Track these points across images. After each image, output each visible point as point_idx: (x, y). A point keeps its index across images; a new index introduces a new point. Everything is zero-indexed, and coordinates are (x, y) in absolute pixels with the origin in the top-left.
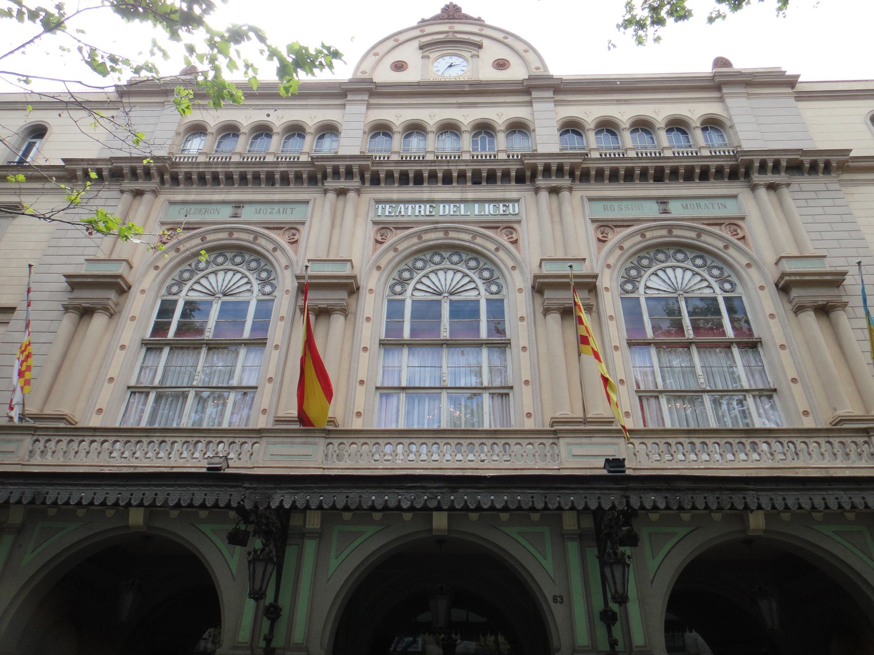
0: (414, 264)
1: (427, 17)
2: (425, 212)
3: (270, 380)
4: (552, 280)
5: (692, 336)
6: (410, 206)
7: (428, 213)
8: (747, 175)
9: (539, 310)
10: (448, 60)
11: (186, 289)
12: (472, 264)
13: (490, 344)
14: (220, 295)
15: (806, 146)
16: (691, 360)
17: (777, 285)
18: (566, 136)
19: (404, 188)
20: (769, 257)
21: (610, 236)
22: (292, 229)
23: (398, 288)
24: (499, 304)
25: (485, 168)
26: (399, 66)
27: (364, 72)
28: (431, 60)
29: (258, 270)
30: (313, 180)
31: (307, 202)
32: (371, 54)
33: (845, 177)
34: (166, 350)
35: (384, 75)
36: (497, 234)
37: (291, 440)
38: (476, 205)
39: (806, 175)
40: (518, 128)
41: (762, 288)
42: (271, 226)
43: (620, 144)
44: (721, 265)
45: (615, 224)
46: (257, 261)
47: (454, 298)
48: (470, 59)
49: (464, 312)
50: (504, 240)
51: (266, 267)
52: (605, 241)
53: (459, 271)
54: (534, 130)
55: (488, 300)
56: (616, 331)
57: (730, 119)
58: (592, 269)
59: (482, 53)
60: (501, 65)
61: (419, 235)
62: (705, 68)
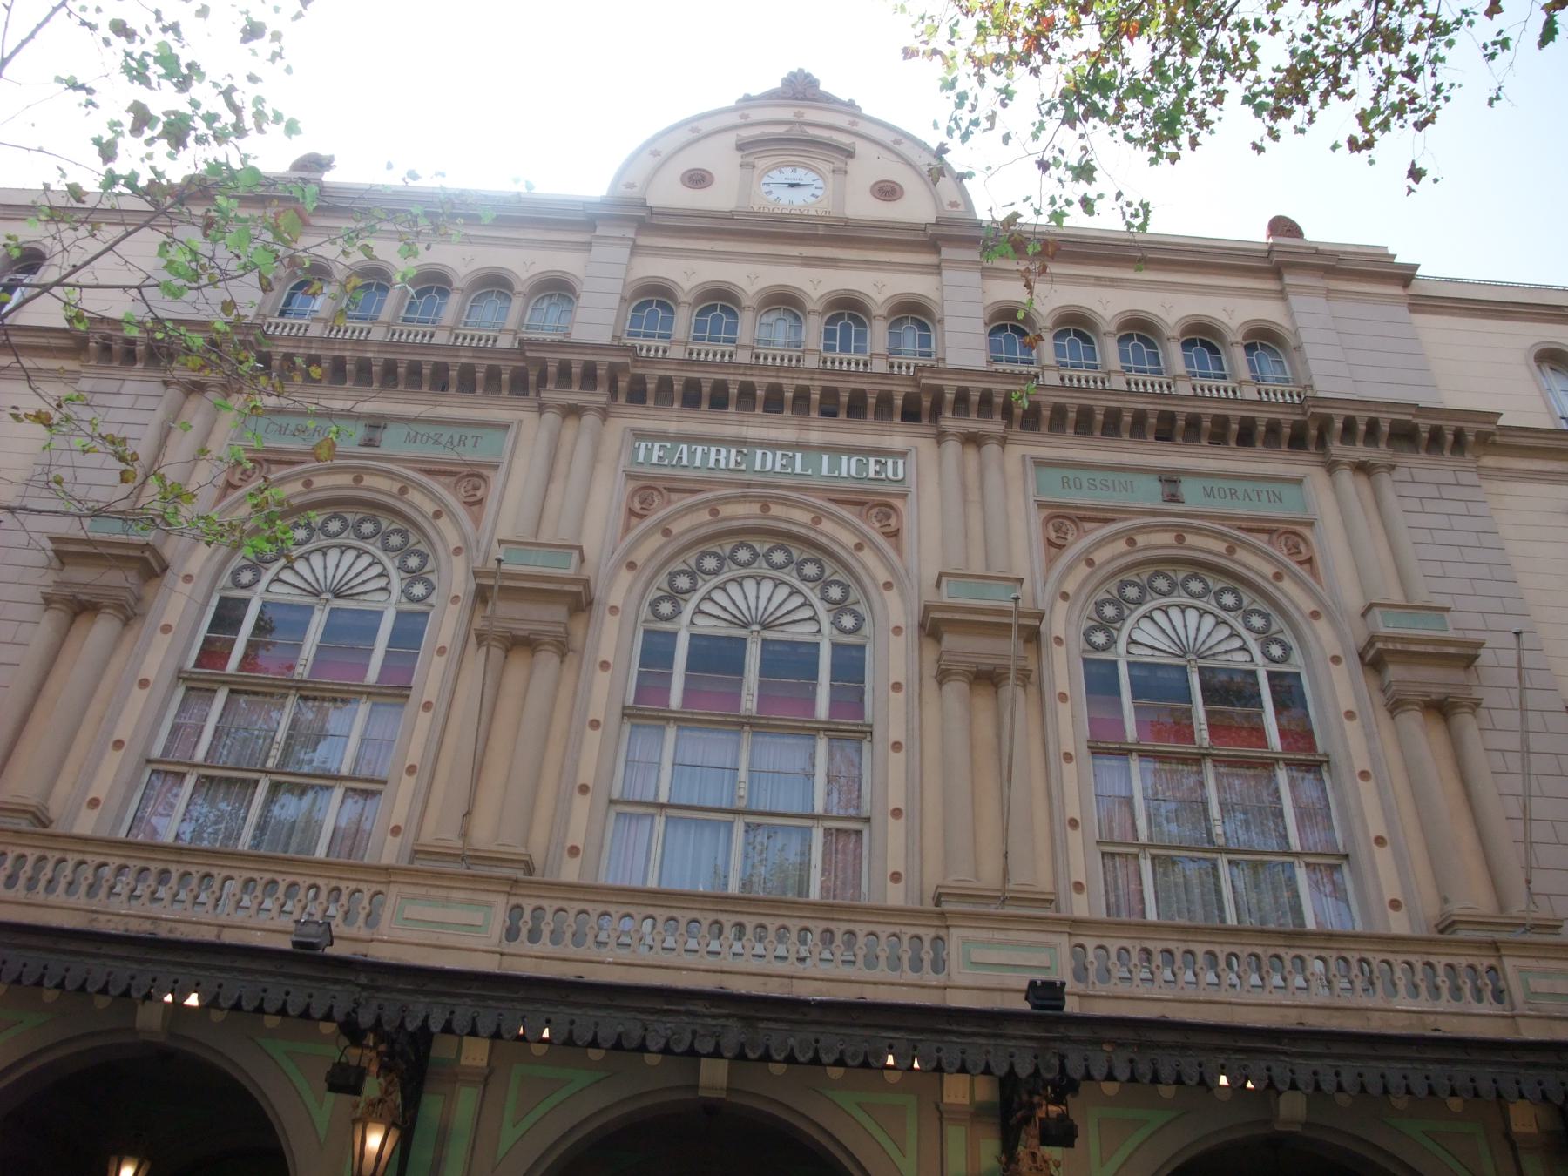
0: (698, 562)
1: (755, 92)
2: (727, 463)
3: (411, 770)
4: (957, 616)
5: (1206, 744)
6: (699, 449)
7: (732, 465)
8: (1322, 442)
9: (930, 670)
10: (789, 175)
11: (266, 577)
12: (810, 570)
13: (834, 733)
14: (329, 596)
15: (1424, 399)
16: (1202, 784)
17: (1361, 656)
18: (1001, 337)
20: (1353, 600)
21: (1070, 537)
22: (472, 481)
23: (666, 608)
24: (854, 653)
25: (845, 387)
26: (698, 179)
27: (631, 186)
28: (756, 172)
29: (404, 551)
30: (520, 385)
31: (505, 427)
33: (1489, 461)
34: (222, 695)
36: (860, 516)
38: (825, 458)
39: (1423, 454)
40: (913, 314)
41: (1336, 660)
42: (437, 467)
43: (1099, 362)
44: (1266, 608)
45: (1081, 513)
46: (403, 534)
47: (771, 635)
48: (830, 175)
49: (789, 664)
50: (873, 531)
51: (418, 547)
52: (1060, 547)
54: (941, 321)
56: (1071, 723)
57: (1296, 333)
58: (1035, 600)
59: (852, 165)
60: (887, 191)
62: (1256, 233)
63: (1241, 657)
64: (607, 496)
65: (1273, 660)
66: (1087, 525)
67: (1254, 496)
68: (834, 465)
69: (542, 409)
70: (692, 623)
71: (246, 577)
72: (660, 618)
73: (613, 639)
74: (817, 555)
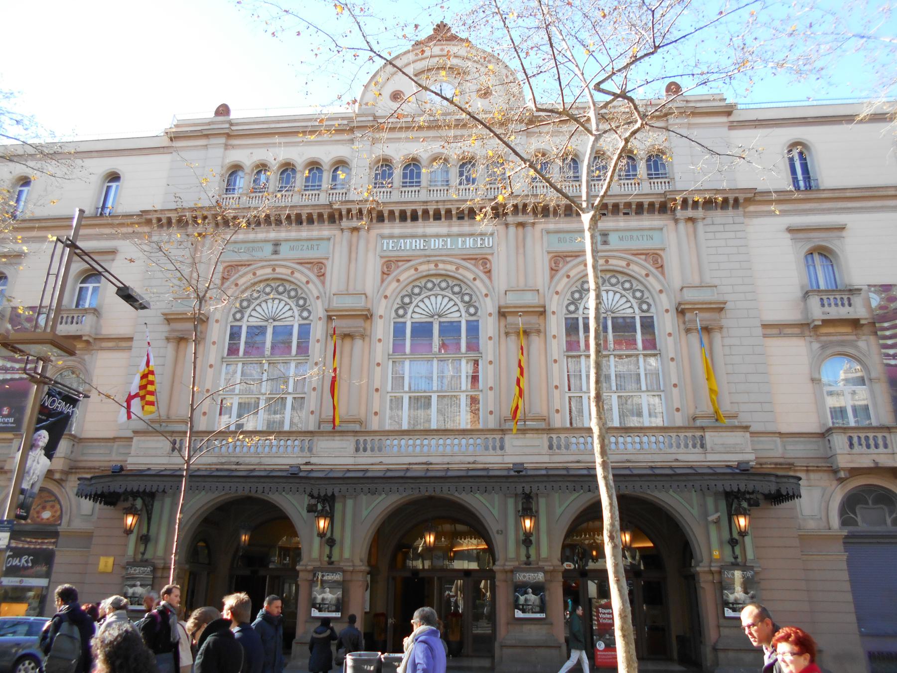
0: (412, 290)
3: (314, 389)
9: (503, 330)
17: (677, 309)
20: (677, 283)
21: (561, 265)
22: (319, 267)
23: (401, 312)
33: (752, 208)
36: (475, 265)
47: (442, 320)
49: (450, 329)
55: (467, 321)
63: (631, 310)
64: (372, 266)
65: (643, 311)
66: (568, 259)
67: (641, 238)
68: (464, 242)
71: (238, 316)
73: (382, 329)
74: (459, 282)
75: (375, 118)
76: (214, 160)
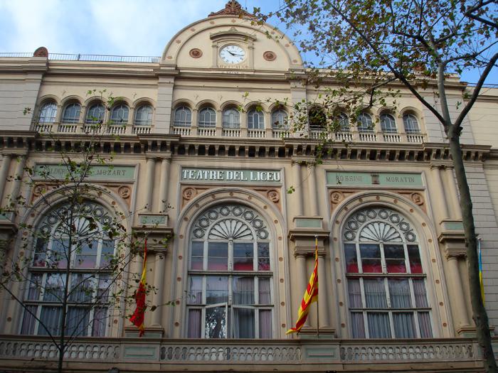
1: (216, 11)
5: (386, 273)
7: (218, 178)
12: (249, 216)
17: (438, 240)
19: (202, 158)
32: (175, 42)
33: (488, 162)
35: (186, 62)
37: (139, 345)
38: (252, 173)
42: (110, 184)
45: (343, 190)
47: (236, 241)
50: (270, 201)
53: (239, 221)
55: (258, 243)
56: (340, 269)
61: (212, 194)
68: (255, 176)
69: (147, 159)
70: (209, 238)
72: (197, 237)
75: (177, 69)
76: (28, 91)
